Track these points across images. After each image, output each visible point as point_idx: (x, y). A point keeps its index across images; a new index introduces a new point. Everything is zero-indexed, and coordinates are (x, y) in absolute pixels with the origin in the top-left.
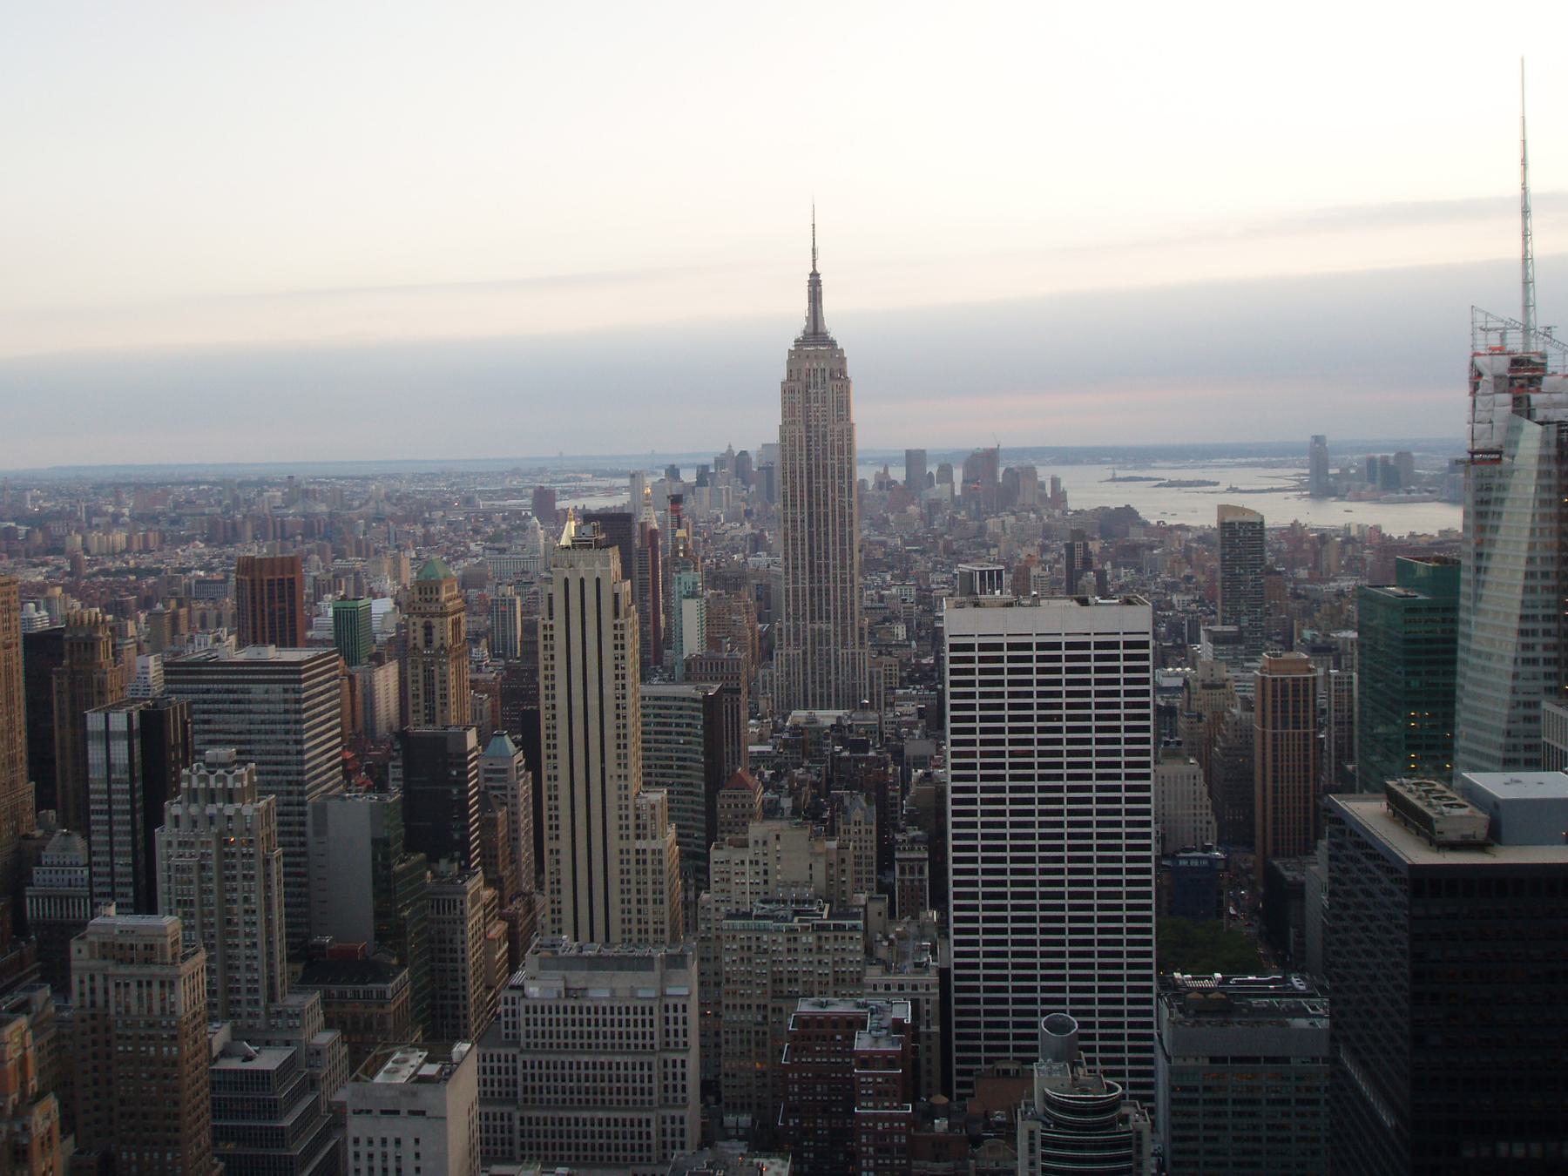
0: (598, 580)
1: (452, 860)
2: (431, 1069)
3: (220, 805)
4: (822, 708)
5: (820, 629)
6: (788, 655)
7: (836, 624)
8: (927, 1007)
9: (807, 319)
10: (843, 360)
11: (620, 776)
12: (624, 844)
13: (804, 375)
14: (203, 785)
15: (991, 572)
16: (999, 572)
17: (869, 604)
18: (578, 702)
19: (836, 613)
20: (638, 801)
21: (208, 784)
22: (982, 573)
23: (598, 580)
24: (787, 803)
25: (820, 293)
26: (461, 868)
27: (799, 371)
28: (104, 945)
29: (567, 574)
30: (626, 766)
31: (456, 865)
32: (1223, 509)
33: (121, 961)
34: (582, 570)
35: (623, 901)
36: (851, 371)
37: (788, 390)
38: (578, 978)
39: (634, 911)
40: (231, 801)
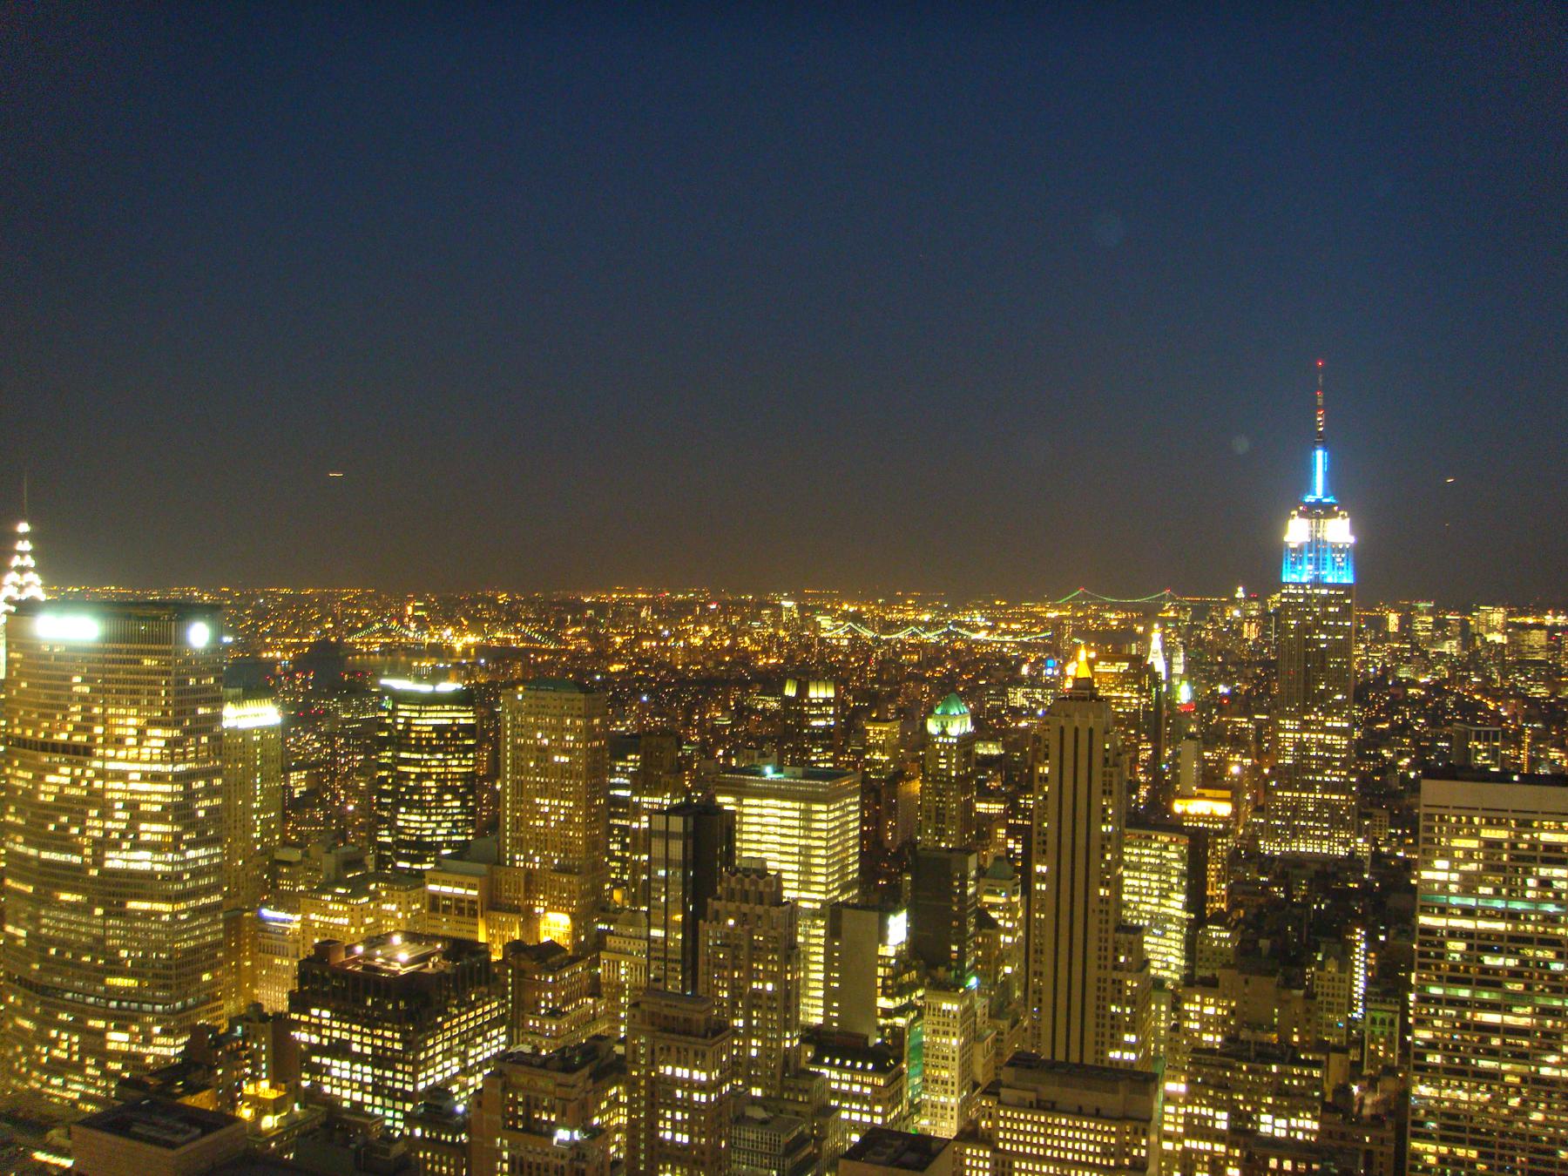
0: (1091, 731)
1: (949, 969)
2: (911, 1157)
3: (752, 905)
8: (1380, 1159)
11: (1101, 911)
12: (1102, 973)
14: (739, 887)
18: (1066, 840)
20: (1117, 935)
21: (743, 885)
23: (1091, 731)
24: (1264, 943)
26: (956, 976)
28: (653, 1014)
29: (1063, 723)
30: (1107, 903)
31: (953, 973)
33: (665, 1030)
34: (1077, 720)
35: (1097, 1025)
38: (1050, 1091)
39: (1108, 1034)
40: (761, 903)
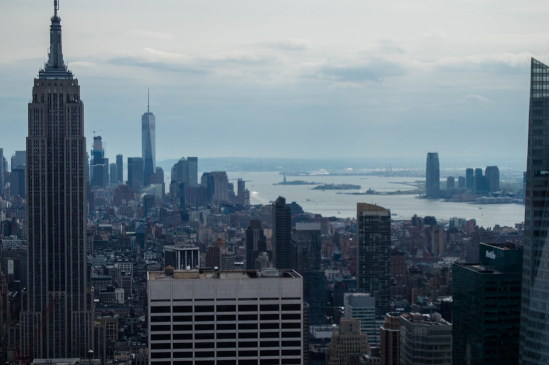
4: (57, 357)
5: (57, 297)
6: (31, 316)
7: (69, 291)
9: (50, 55)
10: (77, 88)
13: (46, 99)
15: (189, 252)
16: (196, 252)
17: (94, 275)
19: (69, 284)
22: (183, 252)
25: (59, 36)
27: (43, 97)
32: (361, 207)
36: (83, 96)
37: (33, 110)
